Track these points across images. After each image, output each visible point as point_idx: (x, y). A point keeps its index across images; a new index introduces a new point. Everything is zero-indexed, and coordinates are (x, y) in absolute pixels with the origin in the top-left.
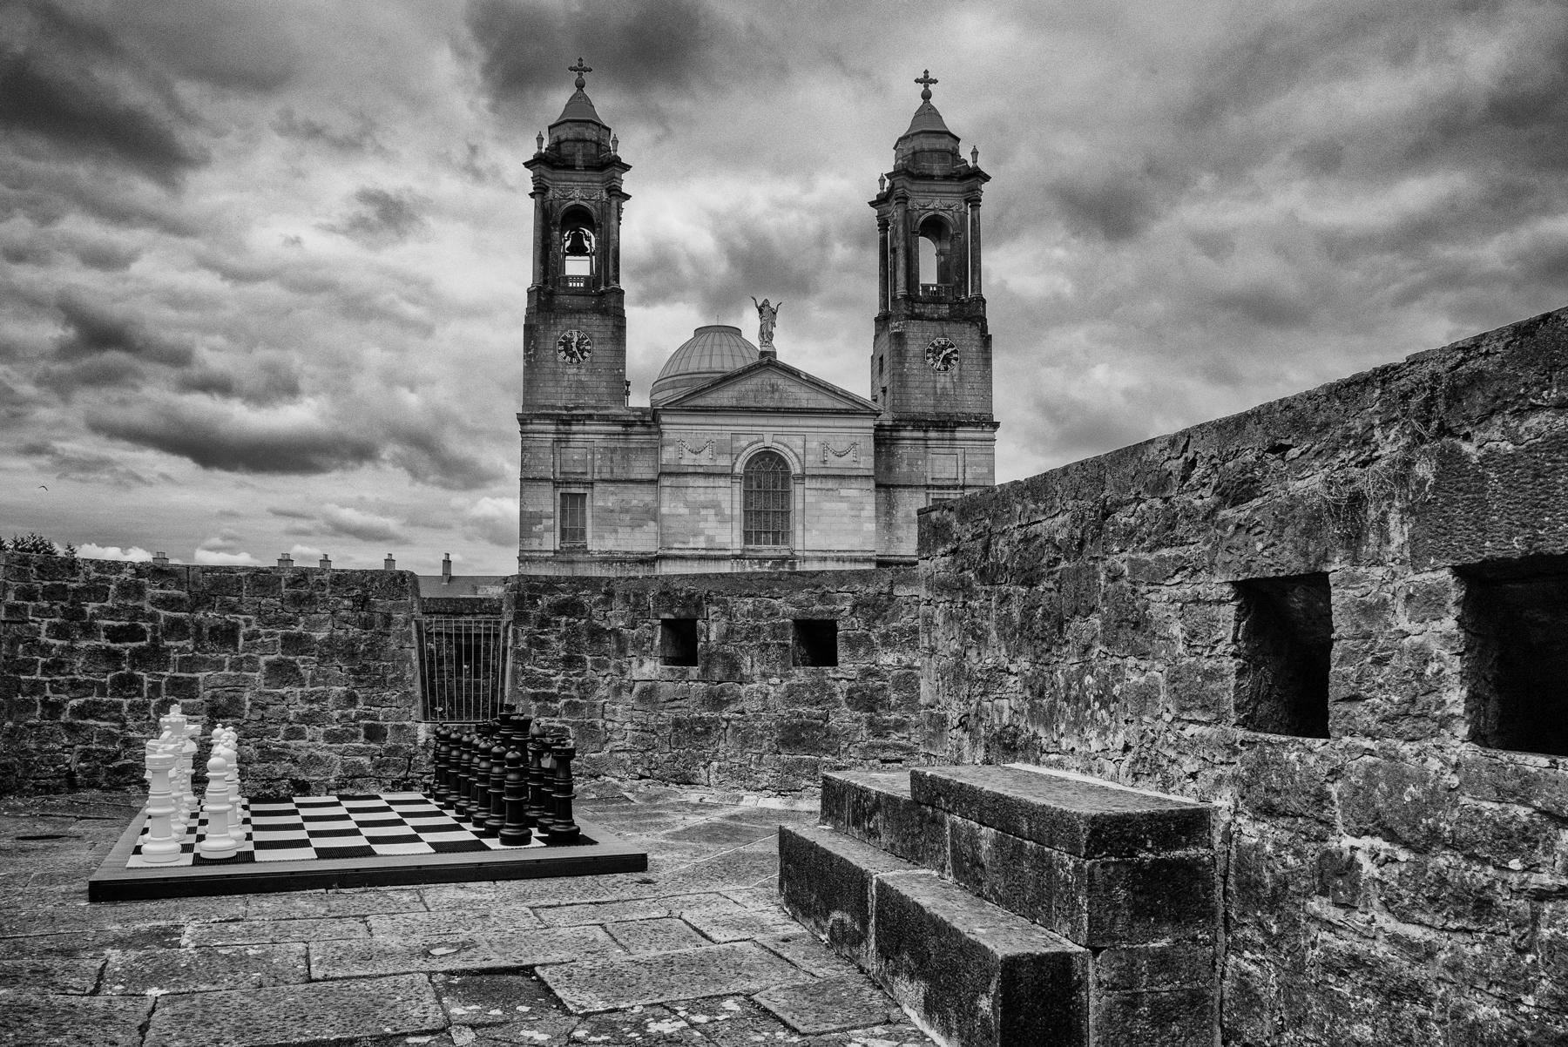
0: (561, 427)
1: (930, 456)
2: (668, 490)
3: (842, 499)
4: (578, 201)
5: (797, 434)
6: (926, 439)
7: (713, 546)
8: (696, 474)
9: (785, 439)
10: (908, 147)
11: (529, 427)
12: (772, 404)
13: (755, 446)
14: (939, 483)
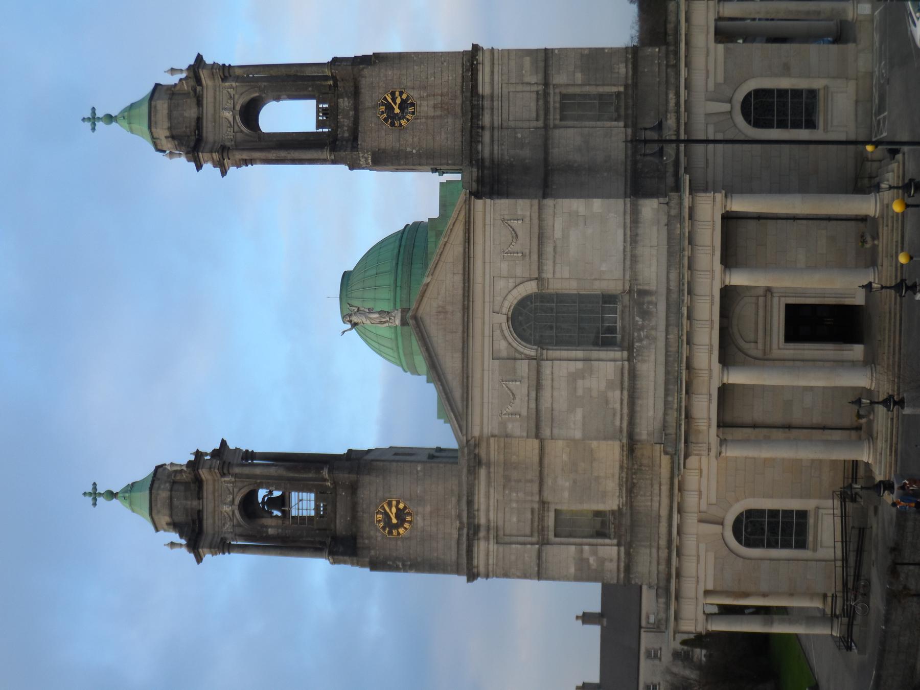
0: (482, 534)
1: (512, 124)
2: (556, 431)
3: (565, 237)
4: (236, 508)
5: (493, 287)
6: (492, 128)
7: (618, 382)
8: (537, 399)
9: (498, 299)
10: (168, 145)
11: (482, 569)
12: (459, 315)
13: (507, 333)
14: (542, 113)
